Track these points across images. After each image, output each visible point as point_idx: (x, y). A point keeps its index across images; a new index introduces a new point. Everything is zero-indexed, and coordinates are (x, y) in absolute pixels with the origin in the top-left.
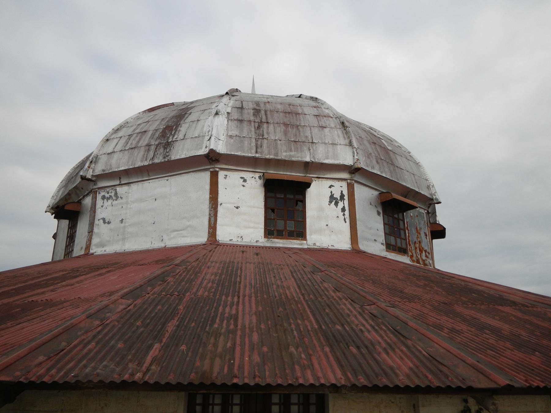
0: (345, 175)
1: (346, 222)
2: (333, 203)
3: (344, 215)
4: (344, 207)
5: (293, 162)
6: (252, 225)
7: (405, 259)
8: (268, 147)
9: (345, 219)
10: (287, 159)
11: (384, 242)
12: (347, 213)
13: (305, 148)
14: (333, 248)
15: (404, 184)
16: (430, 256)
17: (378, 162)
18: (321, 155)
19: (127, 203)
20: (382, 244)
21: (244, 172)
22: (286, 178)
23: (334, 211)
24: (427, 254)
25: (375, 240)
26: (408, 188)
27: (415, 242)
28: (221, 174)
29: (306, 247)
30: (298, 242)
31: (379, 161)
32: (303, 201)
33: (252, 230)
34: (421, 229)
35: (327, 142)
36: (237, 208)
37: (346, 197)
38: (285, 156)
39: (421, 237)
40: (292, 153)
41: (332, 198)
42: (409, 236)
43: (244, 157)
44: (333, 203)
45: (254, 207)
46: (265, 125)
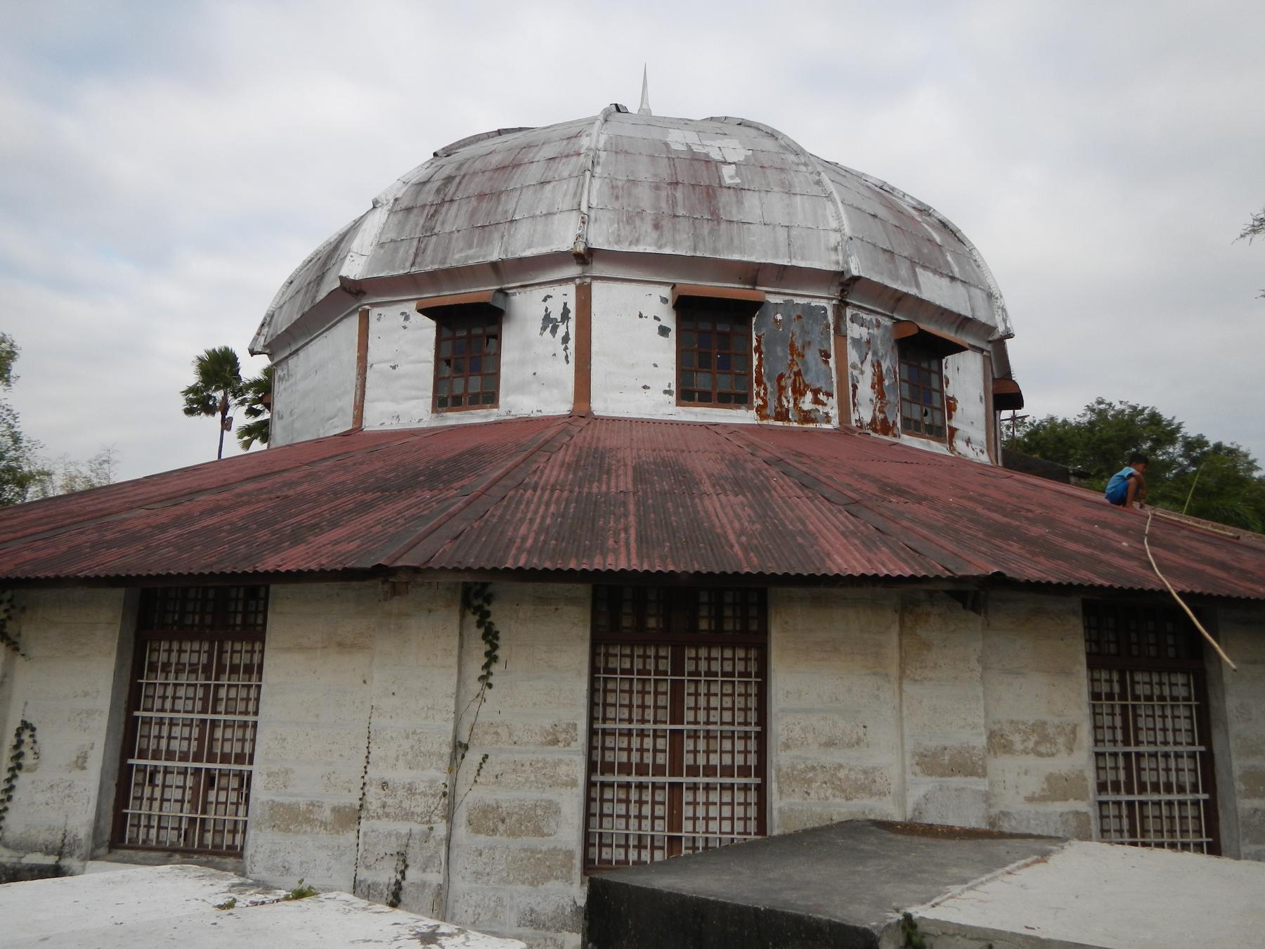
0: (573, 270)
1: (568, 362)
2: (549, 330)
3: (566, 349)
4: (567, 333)
5: (471, 267)
6: (414, 393)
7: (743, 417)
8: (434, 250)
9: (567, 357)
10: (460, 265)
11: (674, 388)
12: (572, 344)
13: (496, 236)
14: (540, 414)
15: (736, 257)
16: (833, 402)
17: (657, 226)
18: (524, 243)
19: (296, 383)
20: (665, 392)
21: (406, 304)
22: (448, 302)
23: (553, 343)
24: (821, 397)
25: (645, 387)
26: (749, 263)
27: (781, 376)
28: (374, 313)
29: (492, 419)
30: (483, 412)
31: (666, 223)
32: (497, 337)
33: (414, 402)
34: (807, 344)
35: (538, 213)
36: (394, 368)
37: (572, 315)
38: (458, 261)
39: (805, 363)
40: (471, 252)
41: (547, 319)
42: (759, 366)
43: (392, 277)
44: (549, 330)
45: (420, 362)
46: (446, 206)
